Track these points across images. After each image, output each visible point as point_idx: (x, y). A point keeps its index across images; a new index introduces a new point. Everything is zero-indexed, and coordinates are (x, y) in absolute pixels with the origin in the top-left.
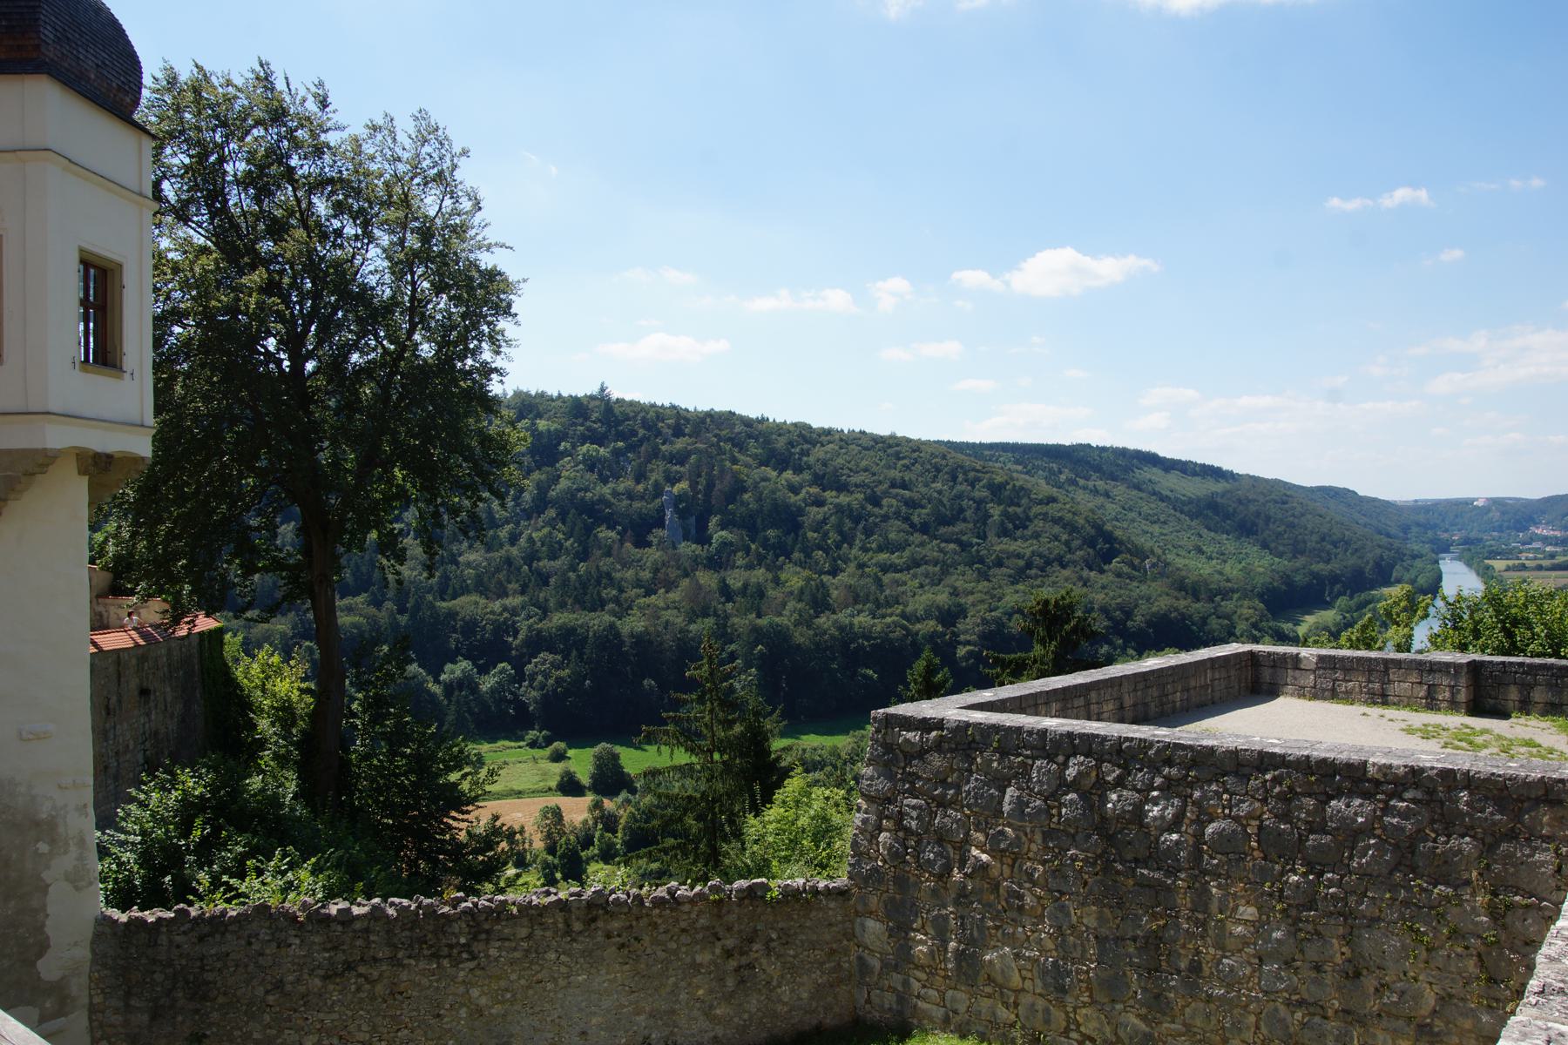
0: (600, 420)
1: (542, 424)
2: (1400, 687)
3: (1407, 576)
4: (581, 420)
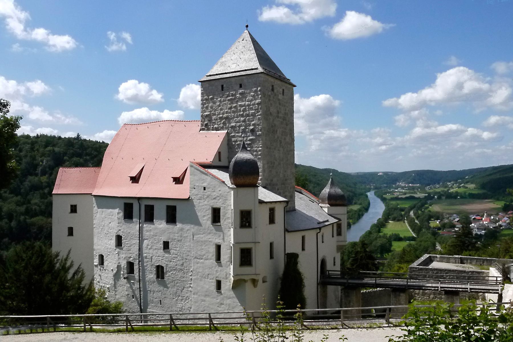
0: (79, 148)
1: (57, 149)
2: (451, 260)
3: (359, 202)
4: (71, 148)
